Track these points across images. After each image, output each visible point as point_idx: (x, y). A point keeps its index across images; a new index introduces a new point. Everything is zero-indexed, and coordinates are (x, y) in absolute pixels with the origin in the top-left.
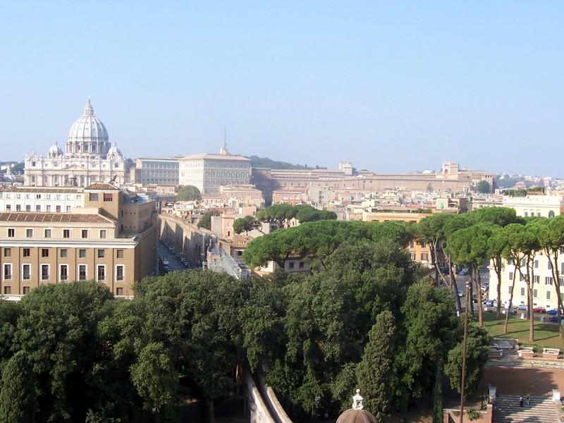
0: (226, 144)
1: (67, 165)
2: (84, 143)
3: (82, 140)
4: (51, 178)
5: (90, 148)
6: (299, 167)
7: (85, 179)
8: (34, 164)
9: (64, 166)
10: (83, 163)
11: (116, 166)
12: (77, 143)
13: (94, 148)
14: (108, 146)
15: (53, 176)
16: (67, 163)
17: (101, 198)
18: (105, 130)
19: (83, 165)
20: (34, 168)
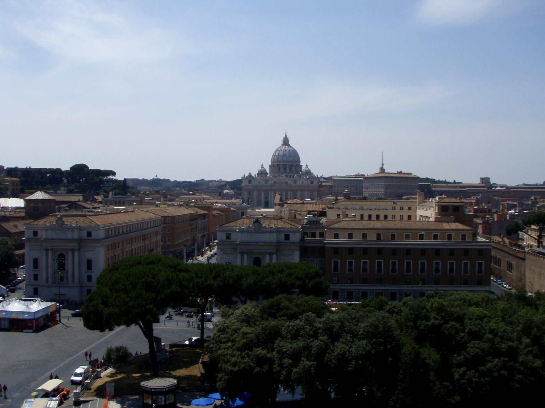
0: (383, 165)
1: (275, 182)
2: (284, 165)
3: (282, 163)
4: (263, 192)
5: (288, 169)
6: (439, 182)
7: (289, 192)
8: (250, 182)
9: (273, 182)
10: (287, 181)
11: (312, 183)
12: (278, 165)
13: (291, 169)
14: (301, 166)
15: (264, 190)
16: (275, 180)
17: (451, 210)
18: (298, 157)
19: (287, 182)
20: (250, 185)
